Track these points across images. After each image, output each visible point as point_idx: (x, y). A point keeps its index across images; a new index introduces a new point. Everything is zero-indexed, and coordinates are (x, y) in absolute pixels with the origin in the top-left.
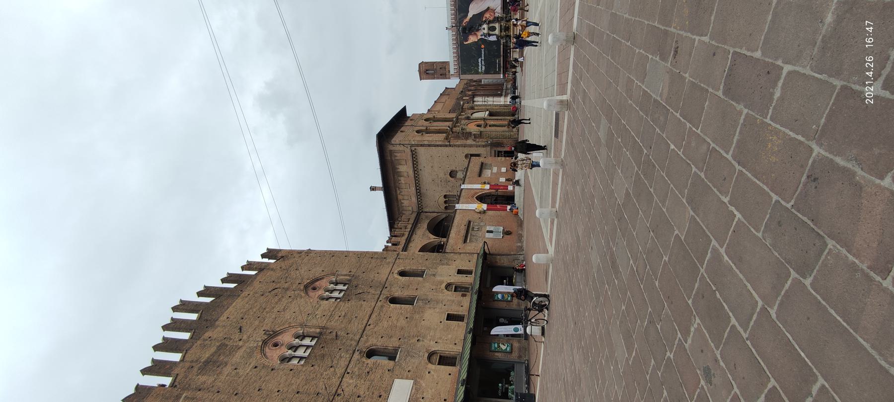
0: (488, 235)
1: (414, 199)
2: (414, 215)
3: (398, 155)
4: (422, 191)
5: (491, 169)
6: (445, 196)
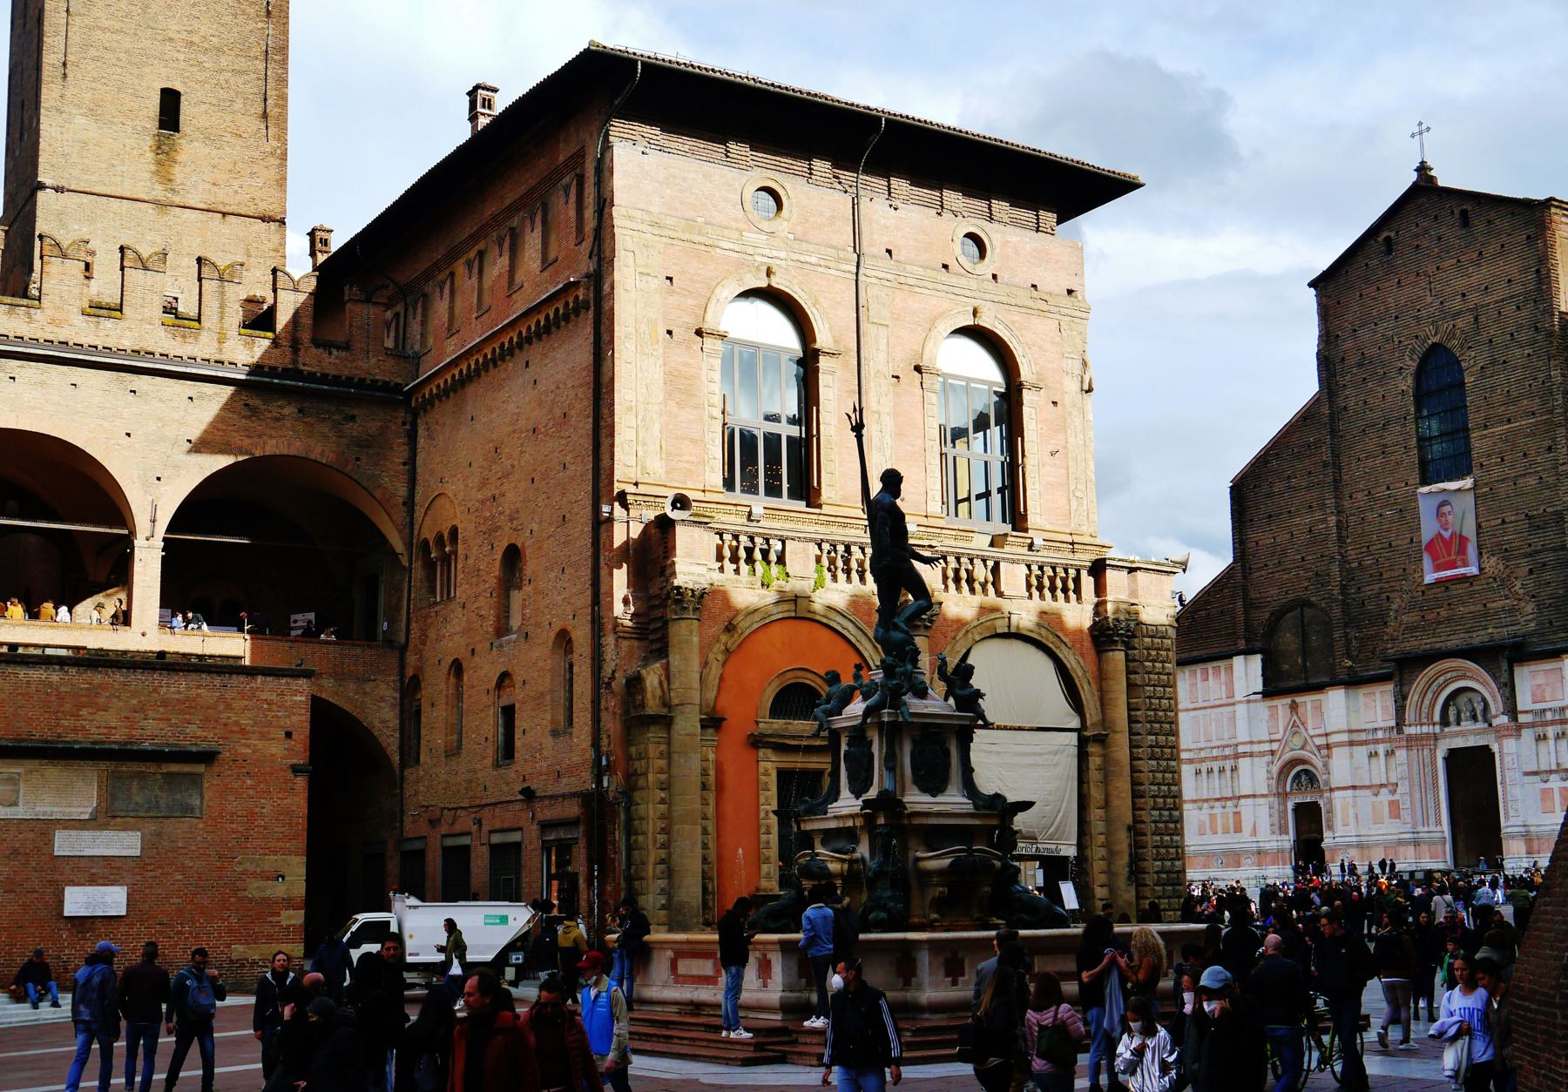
1: (452, 350)
2: (373, 366)
3: (572, 213)
4: (471, 389)
5: (102, 819)
6: (454, 532)
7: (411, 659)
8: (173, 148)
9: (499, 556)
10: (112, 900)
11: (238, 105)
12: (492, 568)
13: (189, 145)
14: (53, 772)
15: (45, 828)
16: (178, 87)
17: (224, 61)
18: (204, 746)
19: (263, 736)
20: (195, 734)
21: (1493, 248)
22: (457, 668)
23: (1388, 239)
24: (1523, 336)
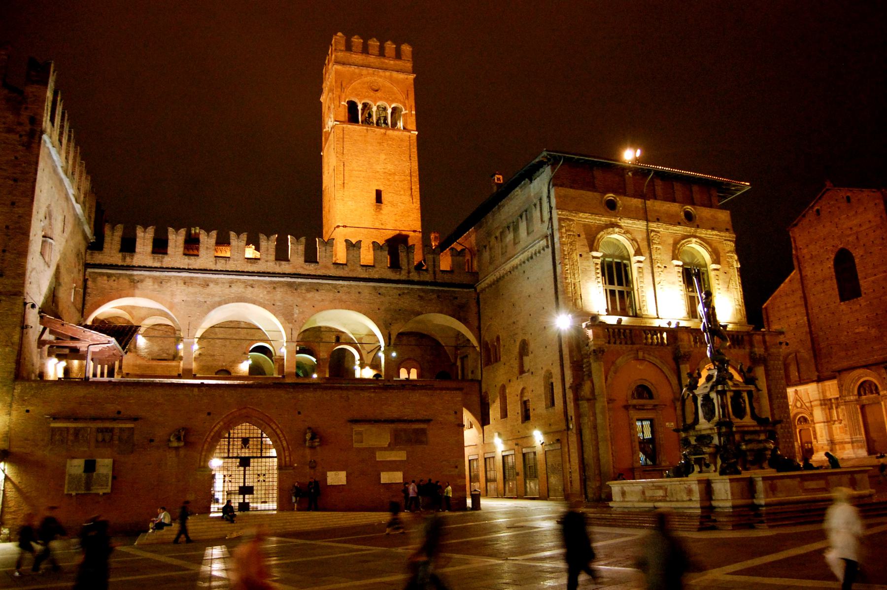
0: (76, 466)
3: (539, 214)
6: (498, 338)
7: (484, 385)
8: (381, 209)
9: (518, 344)
10: (397, 477)
11: (402, 192)
12: (516, 350)
13: (386, 208)
14: (374, 429)
15: (372, 451)
16: (381, 188)
17: (396, 177)
18: (427, 418)
19: (447, 414)
20: (423, 414)
21: (861, 210)
22: (503, 388)
23: (818, 211)
24: (877, 242)
